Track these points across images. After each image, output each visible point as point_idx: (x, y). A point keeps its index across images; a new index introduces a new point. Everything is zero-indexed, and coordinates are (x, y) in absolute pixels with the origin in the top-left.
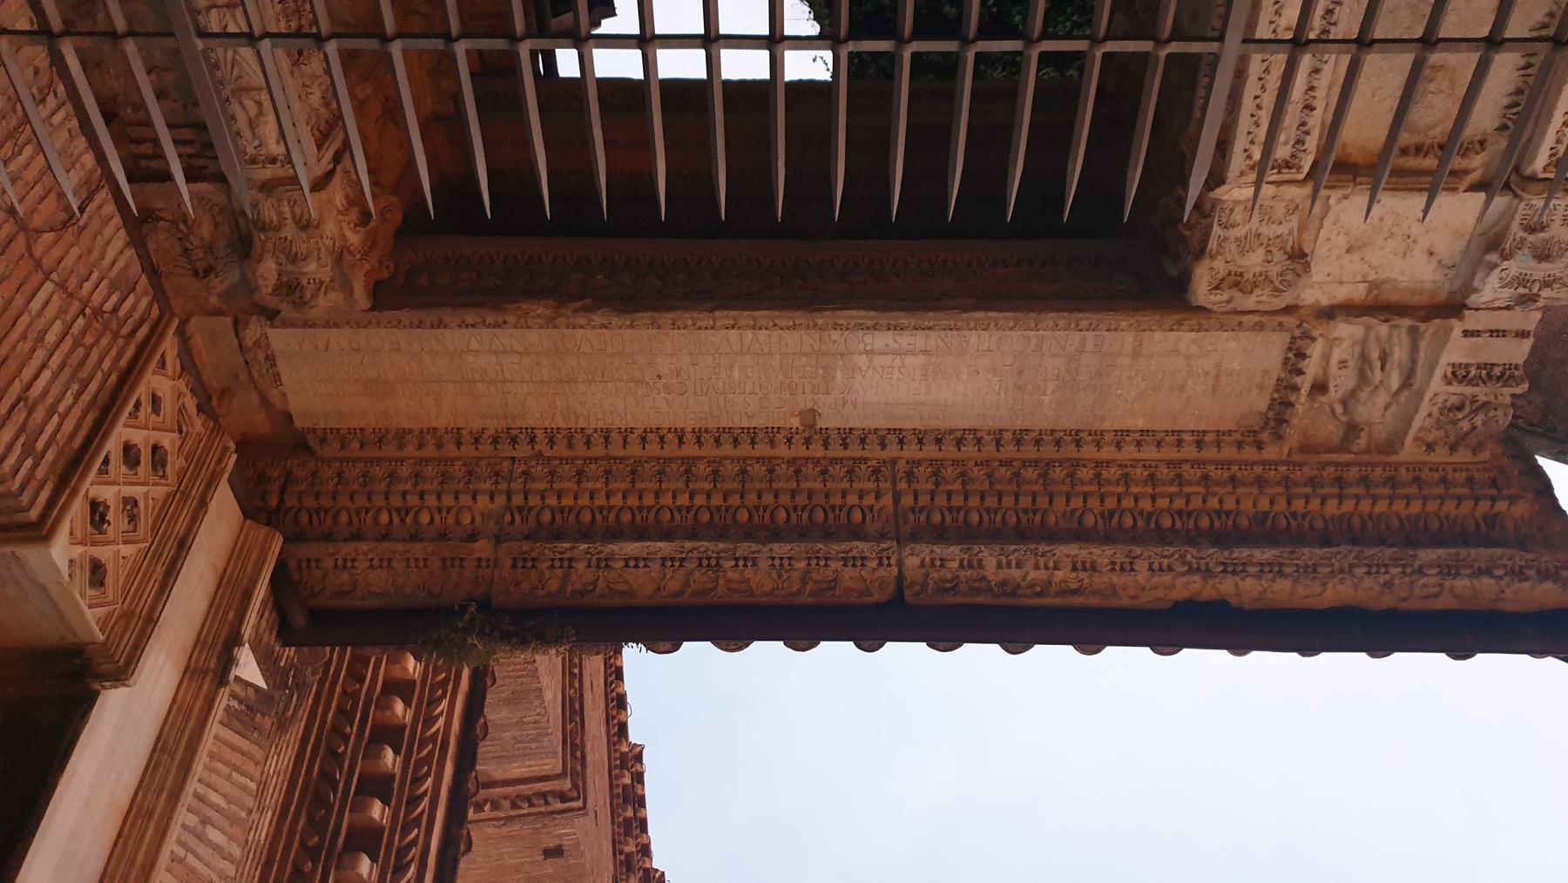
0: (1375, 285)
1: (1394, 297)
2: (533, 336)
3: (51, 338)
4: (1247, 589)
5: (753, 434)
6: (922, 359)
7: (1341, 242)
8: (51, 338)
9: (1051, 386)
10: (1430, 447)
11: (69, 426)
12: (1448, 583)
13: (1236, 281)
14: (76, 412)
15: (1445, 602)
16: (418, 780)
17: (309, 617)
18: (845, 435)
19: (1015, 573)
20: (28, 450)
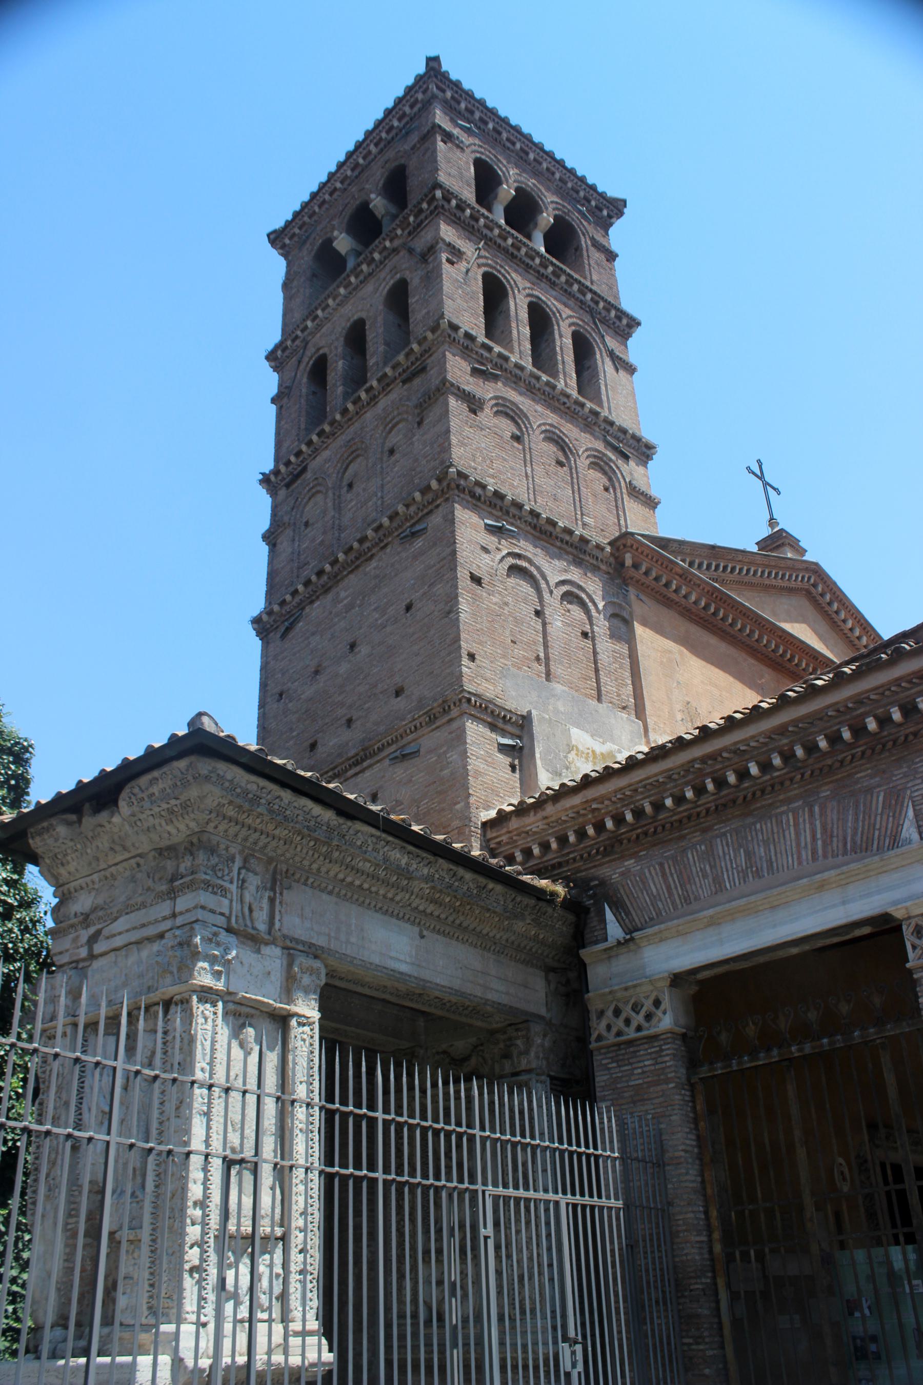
0: (258, 951)
1: (249, 942)
2: (489, 996)
3: (640, 1071)
4: (328, 815)
5: (439, 932)
6: (393, 954)
7: (273, 978)
8: (640, 1071)
9: (353, 927)
10: (227, 849)
11: (646, 1046)
12: (258, 793)
13: (312, 971)
14: (642, 1047)
15: (263, 782)
16: (565, 822)
17: (581, 915)
18: (413, 923)
19: (398, 856)
20: (662, 1050)
